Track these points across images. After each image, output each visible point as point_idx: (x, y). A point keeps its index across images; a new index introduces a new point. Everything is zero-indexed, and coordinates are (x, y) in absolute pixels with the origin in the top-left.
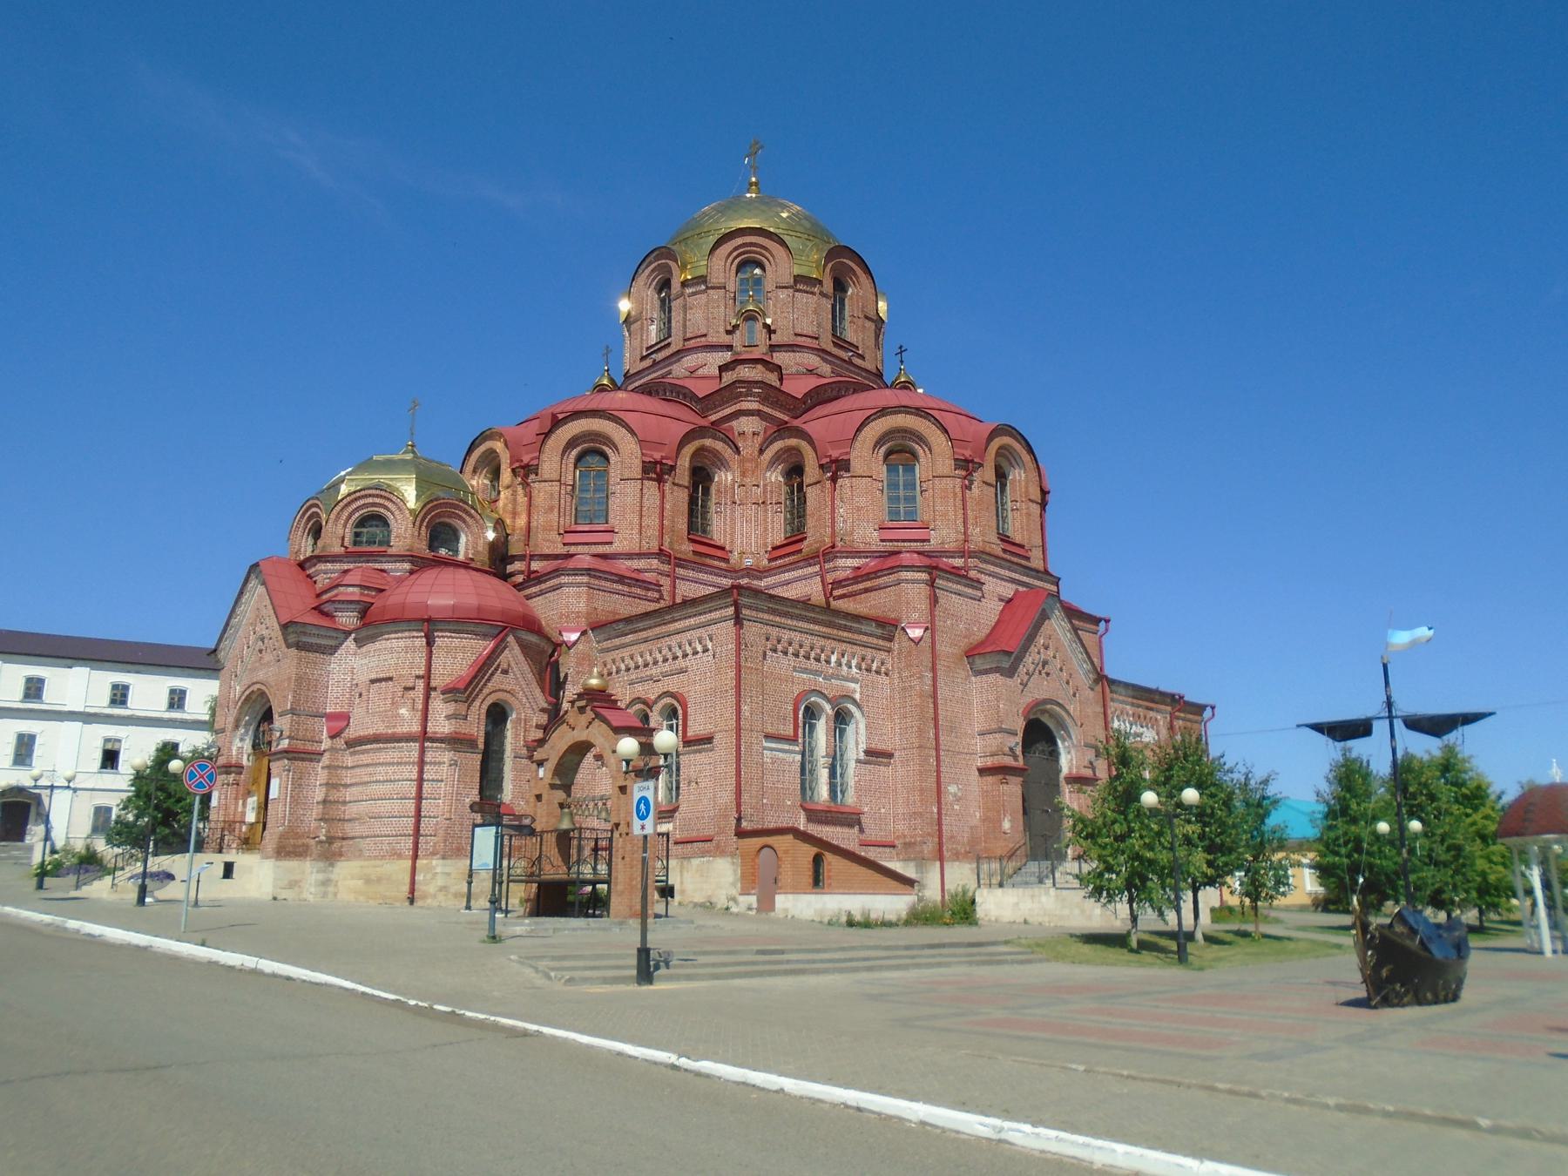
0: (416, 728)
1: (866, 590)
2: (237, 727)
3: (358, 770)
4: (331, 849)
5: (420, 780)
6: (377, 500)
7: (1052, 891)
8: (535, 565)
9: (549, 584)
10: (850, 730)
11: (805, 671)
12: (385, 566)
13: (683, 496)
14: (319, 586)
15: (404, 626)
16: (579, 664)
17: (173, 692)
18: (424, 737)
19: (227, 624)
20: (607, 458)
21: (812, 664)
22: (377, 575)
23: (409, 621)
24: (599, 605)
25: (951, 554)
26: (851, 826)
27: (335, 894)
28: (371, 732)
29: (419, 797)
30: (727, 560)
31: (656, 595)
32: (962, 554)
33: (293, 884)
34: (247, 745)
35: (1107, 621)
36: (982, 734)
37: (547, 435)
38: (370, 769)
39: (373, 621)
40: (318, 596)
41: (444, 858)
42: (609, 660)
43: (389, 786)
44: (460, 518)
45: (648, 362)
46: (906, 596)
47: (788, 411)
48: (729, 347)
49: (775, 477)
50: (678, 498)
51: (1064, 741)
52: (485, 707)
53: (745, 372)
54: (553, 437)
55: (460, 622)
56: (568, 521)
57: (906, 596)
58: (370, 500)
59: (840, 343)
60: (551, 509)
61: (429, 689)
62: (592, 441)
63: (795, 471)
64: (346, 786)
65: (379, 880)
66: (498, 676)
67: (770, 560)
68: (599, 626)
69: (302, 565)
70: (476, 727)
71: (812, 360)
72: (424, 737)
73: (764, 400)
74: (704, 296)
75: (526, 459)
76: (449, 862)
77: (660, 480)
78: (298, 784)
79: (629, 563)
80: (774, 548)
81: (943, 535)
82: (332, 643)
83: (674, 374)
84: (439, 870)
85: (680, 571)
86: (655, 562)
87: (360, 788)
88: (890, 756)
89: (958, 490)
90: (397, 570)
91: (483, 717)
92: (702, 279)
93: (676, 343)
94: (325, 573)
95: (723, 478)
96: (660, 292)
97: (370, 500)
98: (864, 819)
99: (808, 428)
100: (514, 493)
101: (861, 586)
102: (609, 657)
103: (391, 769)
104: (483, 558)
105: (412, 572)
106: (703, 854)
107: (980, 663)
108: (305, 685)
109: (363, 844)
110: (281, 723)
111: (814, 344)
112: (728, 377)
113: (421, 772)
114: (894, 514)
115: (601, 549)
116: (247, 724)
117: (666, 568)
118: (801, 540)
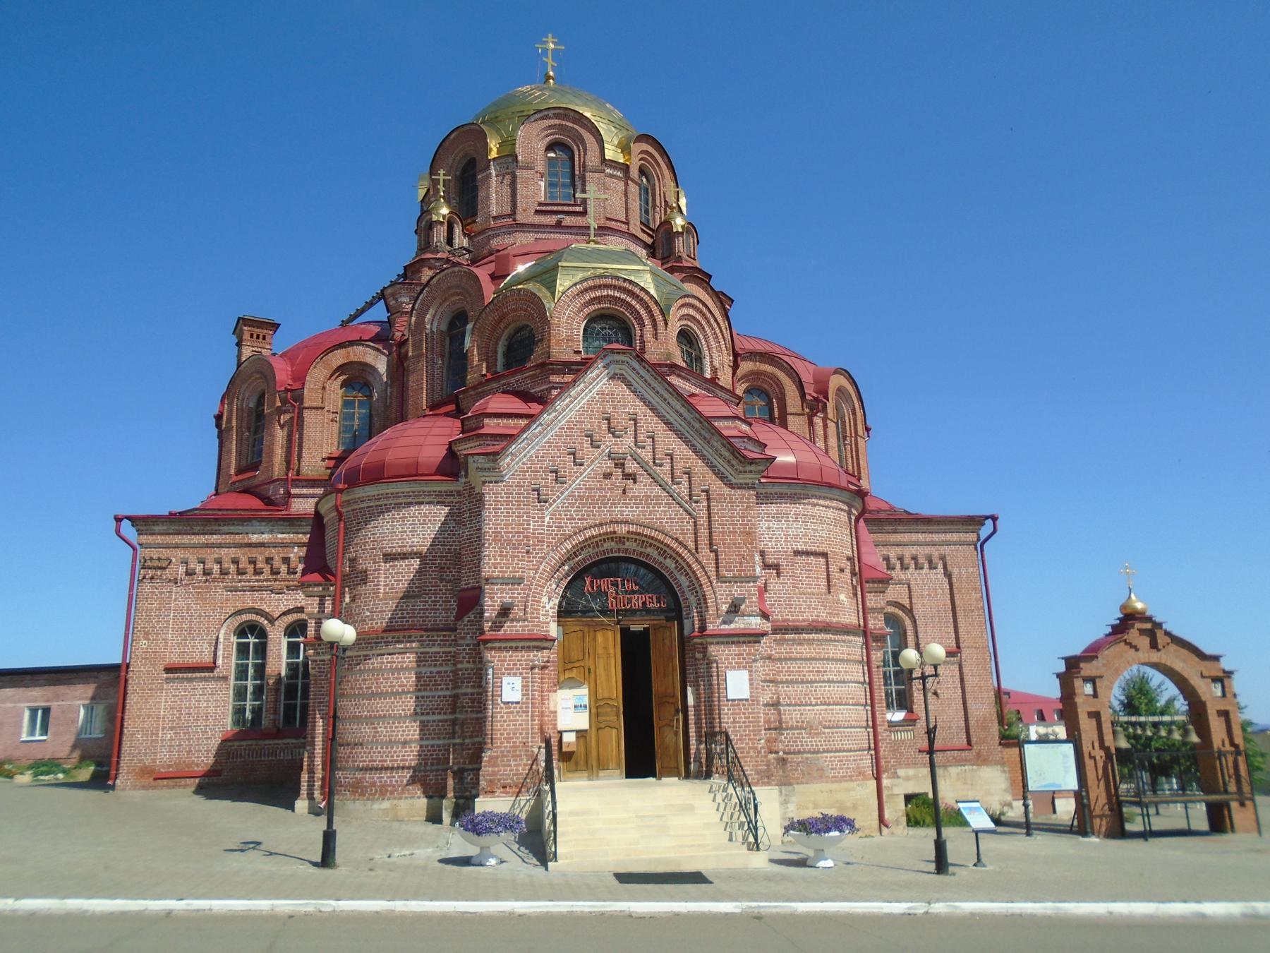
3: (794, 666)
38: (818, 665)
96: (550, 148)
103: (842, 667)
106: (962, 762)
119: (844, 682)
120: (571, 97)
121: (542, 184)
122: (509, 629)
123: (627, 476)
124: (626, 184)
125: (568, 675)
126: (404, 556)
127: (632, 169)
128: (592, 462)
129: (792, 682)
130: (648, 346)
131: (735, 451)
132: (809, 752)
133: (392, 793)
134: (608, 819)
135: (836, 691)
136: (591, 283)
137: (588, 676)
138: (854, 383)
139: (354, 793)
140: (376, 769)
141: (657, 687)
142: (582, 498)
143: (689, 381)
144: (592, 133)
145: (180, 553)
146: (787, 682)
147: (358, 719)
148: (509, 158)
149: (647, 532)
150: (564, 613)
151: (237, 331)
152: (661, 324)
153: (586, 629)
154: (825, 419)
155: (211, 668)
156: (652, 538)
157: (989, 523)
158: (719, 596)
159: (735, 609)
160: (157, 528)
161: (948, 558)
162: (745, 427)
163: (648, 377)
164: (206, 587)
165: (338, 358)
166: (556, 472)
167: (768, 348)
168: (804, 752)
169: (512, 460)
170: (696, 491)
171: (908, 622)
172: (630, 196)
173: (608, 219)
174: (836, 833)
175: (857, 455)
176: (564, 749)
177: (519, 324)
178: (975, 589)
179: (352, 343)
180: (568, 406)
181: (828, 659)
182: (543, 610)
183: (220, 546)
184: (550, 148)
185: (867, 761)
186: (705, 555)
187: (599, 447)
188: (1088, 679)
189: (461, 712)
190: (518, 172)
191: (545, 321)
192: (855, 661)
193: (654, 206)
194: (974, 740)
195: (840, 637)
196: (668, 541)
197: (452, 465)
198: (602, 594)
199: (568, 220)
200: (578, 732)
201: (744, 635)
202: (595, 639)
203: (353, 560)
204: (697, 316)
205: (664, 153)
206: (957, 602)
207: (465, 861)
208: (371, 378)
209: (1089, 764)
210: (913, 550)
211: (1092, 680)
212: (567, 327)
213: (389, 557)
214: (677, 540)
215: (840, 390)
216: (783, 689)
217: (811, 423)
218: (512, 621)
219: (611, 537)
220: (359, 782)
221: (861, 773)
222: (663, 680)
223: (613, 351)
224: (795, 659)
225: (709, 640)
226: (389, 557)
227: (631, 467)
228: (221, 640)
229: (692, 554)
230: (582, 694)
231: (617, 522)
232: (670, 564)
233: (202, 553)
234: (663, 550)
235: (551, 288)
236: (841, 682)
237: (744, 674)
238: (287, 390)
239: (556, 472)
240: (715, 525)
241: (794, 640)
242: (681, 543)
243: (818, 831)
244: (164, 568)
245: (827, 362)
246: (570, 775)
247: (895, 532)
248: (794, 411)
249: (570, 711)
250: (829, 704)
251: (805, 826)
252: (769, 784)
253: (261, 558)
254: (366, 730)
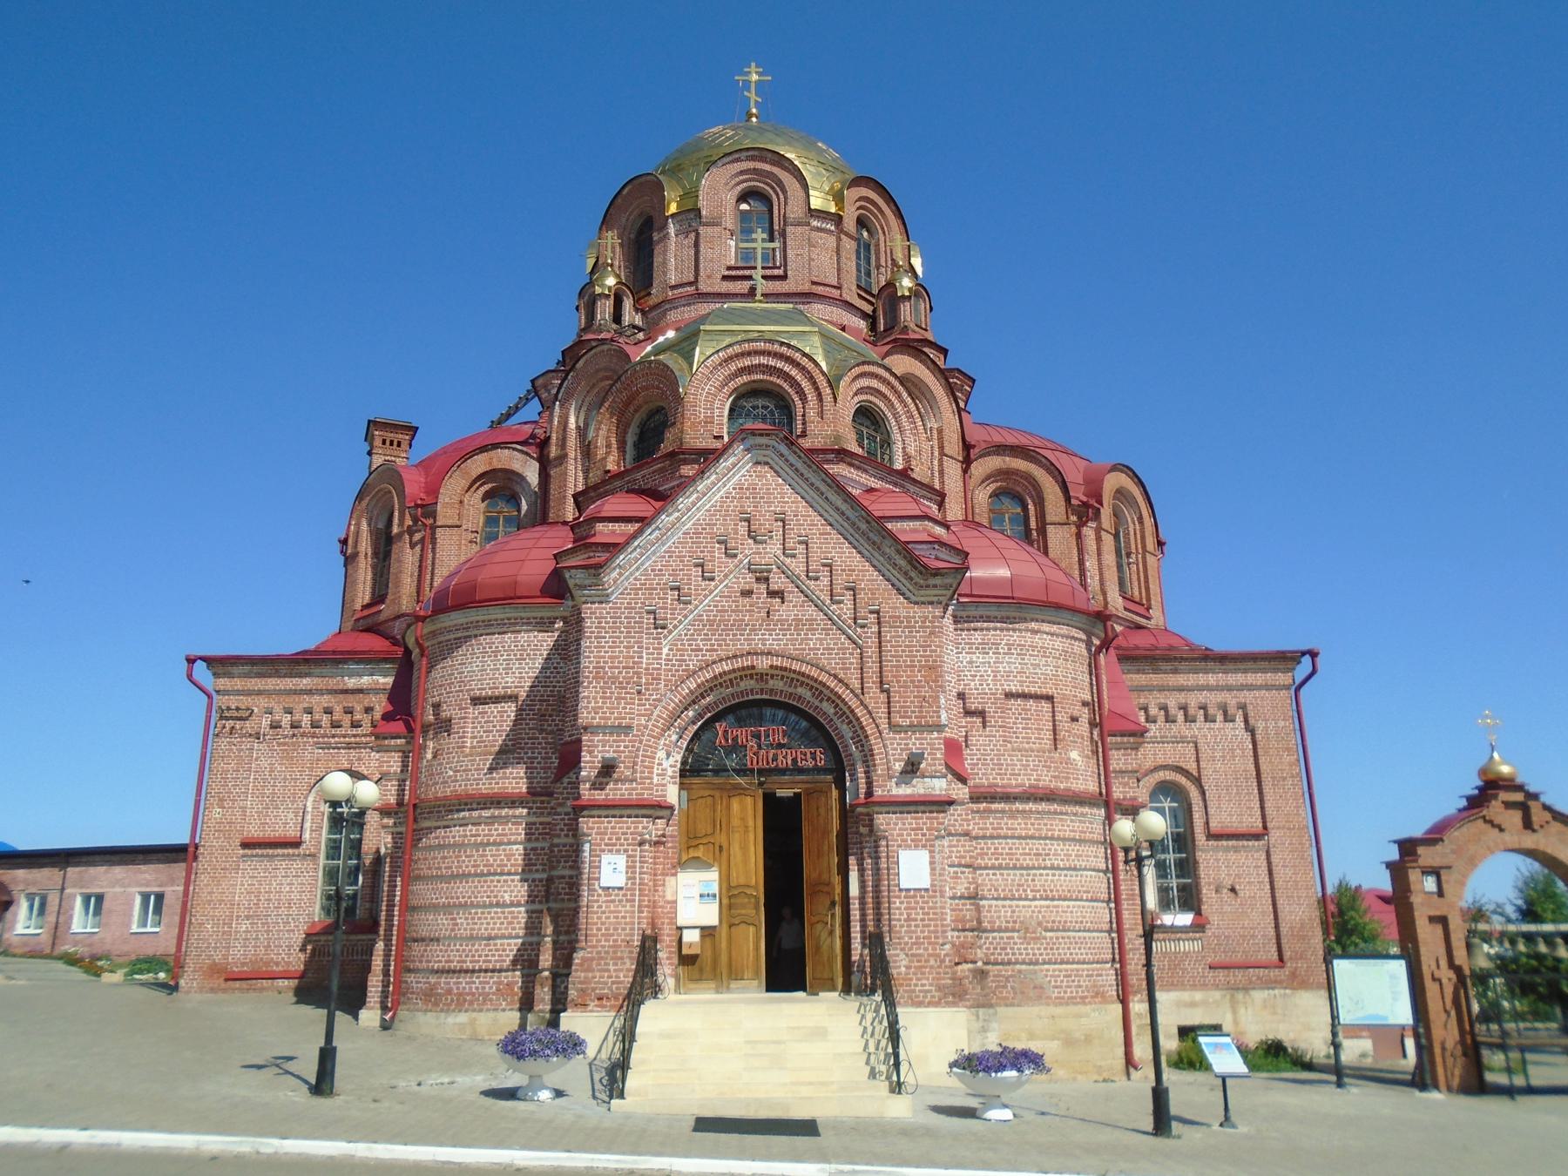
15: (1067, 615)
38: (1038, 845)
65: (1088, 1039)
96: (743, 198)
103: (1073, 849)
106: (1269, 984)
119: (1075, 869)
120: (771, 136)
121: (733, 243)
122: (615, 791)
123: (772, 594)
124: (839, 239)
125: (692, 853)
126: (496, 700)
127: (845, 220)
128: (726, 576)
129: (1000, 867)
130: (811, 427)
131: (913, 560)
132: (1024, 963)
133: (471, 1003)
134: (721, 1043)
135: (1063, 881)
136: (737, 349)
137: (719, 855)
138: (1141, 484)
139: (427, 1001)
140: (454, 972)
141: (809, 871)
142: (711, 623)
143: (865, 471)
144: (788, 171)
145: (263, 702)
146: (993, 868)
147: (435, 908)
148: (691, 215)
149: (796, 666)
150: (689, 771)
151: (369, 437)
152: (828, 398)
153: (717, 794)
154: (1098, 530)
155: (296, 844)
156: (803, 674)
157: (1307, 659)
158: (890, 751)
159: (912, 768)
160: (235, 670)
161: (1250, 708)
162: (939, 530)
163: (799, 465)
164: (293, 744)
165: (479, 464)
166: (678, 589)
167: (1024, 441)
168: (1017, 963)
169: (621, 574)
170: (862, 612)
171: (1194, 793)
172: (843, 254)
173: (814, 283)
174: (1014, 1073)
175: (1146, 577)
176: (685, 951)
177: (652, 406)
178: (1288, 749)
179: (495, 446)
180: (694, 504)
181: (1052, 838)
182: (661, 771)
183: (310, 692)
184: (743, 198)
185: (1109, 977)
186: (874, 697)
187: (735, 556)
188: (1426, 871)
189: (555, 901)
190: (702, 230)
191: (679, 400)
192: (1097, 842)
193: (878, 267)
194: (1287, 954)
195: (1069, 809)
196: (824, 678)
197: (556, 587)
198: (735, 747)
200: (703, 928)
201: (923, 803)
202: (728, 807)
203: (437, 706)
204: (883, 388)
205: (890, 200)
206: (1263, 768)
207: (510, 1094)
208: (518, 489)
209: (1431, 989)
210: (1203, 697)
211: (1436, 872)
212: (706, 405)
213: (477, 701)
214: (835, 676)
215: (1120, 493)
216: (984, 877)
217: (1079, 536)
218: (616, 781)
219: (750, 673)
220: (433, 988)
221: (1099, 995)
222: (818, 862)
223: (753, 433)
224: (1006, 837)
225: (876, 809)
226: (477, 701)
227: (778, 581)
228: (309, 809)
229: (856, 696)
230: (710, 879)
231: (756, 654)
232: (828, 708)
233: (289, 701)
234: (819, 689)
235: (689, 358)
236: (1069, 869)
237: (923, 856)
238: (417, 506)
239: (678, 589)
240: (887, 656)
241: (1003, 811)
242: (840, 681)
243: (987, 1070)
244: (246, 719)
245: (1102, 459)
246: (692, 986)
247: (1175, 671)
248: (1057, 519)
249: (695, 900)
250: (1053, 899)
251: (971, 1064)
252: (954, 1004)
253: (358, 708)
254: (443, 921)
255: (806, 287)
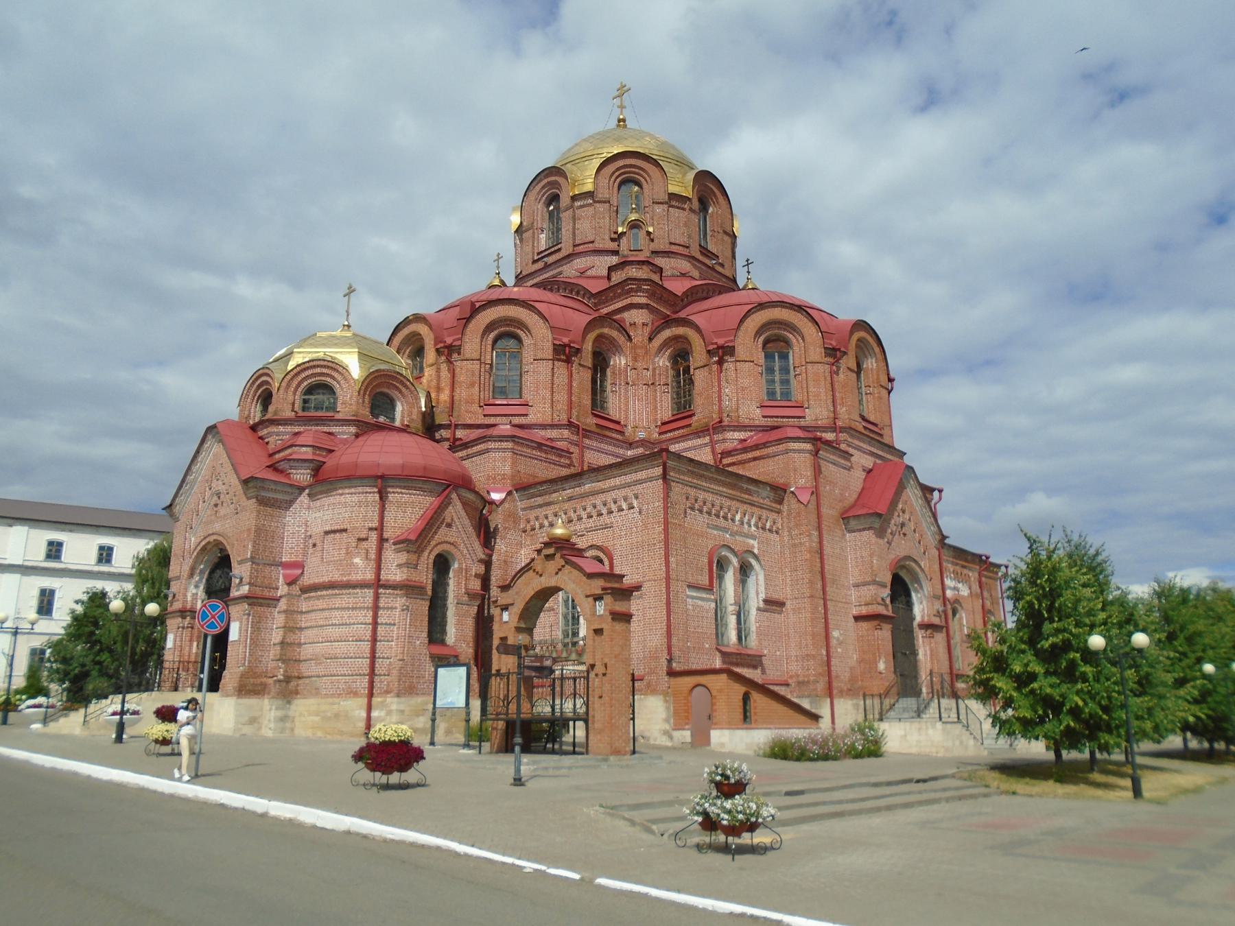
0: (369, 576)
1: (755, 459)
2: (191, 575)
3: (313, 615)
4: (289, 687)
5: (375, 624)
6: (325, 371)
7: (939, 725)
8: (460, 433)
9: (475, 449)
10: (751, 581)
11: (716, 527)
12: (334, 429)
13: (587, 375)
14: (271, 447)
15: (358, 482)
16: (505, 520)
17: (101, 548)
18: (378, 584)
19: (183, 481)
20: (519, 340)
21: (721, 522)
22: (325, 437)
23: (362, 477)
24: (521, 468)
25: (824, 429)
26: (755, 667)
27: (292, 730)
28: (326, 579)
29: (374, 640)
30: (622, 433)
31: (567, 462)
32: (834, 428)
33: (253, 721)
34: (201, 592)
35: (940, 491)
36: (857, 586)
37: (468, 320)
38: (326, 613)
39: (325, 479)
40: (271, 455)
41: (398, 696)
42: (532, 517)
43: (344, 629)
44: (397, 388)
45: (540, 265)
46: (792, 465)
47: (670, 308)
48: (615, 253)
49: (663, 361)
50: (583, 377)
51: (917, 591)
52: (432, 557)
53: (633, 272)
54: (474, 322)
55: (410, 479)
56: (487, 395)
57: (792, 465)
58: (318, 370)
59: (705, 251)
60: (472, 385)
61: (382, 540)
62: (508, 325)
63: (681, 356)
64: (301, 629)
65: (337, 716)
66: (443, 530)
67: (660, 434)
68: (523, 488)
69: (254, 428)
70: (425, 576)
71: (685, 265)
72: (378, 584)
73: (651, 295)
74: (591, 209)
75: (449, 340)
76: (403, 699)
77: (568, 361)
78: (257, 627)
79: (542, 433)
80: (663, 424)
81: (817, 413)
82: (287, 498)
83: (565, 274)
84: (394, 707)
85: (587, 441)
86: (566, 433)
87: (315, 631)
88: (782, 604)
89: (827, 374)
90: (343, 433)
91: (431, 566)
92: (590, 194)
93: (566, 248)
94: (277, 436)
95: (619, 361)
96: (548, 206)
97: (318, 370)
98: (765, 661)
99: (698, 319)
100: (438, 370)
101: (750, 455)
102: (532, 515)
103: (346, 614)
104: (417, 424)
105: (357, 436)
107: (853, 523)
108: (264, 537)
109: (319, 682)
110: (240, 570)
111: (685, 252)
112: (617, 277)
113: (375, 616)
114: (771, 394)
115: (516, 420)
116: (202, 572)
117: (575, 438)
118: (690, 416)
121: (543, 236)
199: (550, 260)
210: (613, 494)
255: (570, 251)
